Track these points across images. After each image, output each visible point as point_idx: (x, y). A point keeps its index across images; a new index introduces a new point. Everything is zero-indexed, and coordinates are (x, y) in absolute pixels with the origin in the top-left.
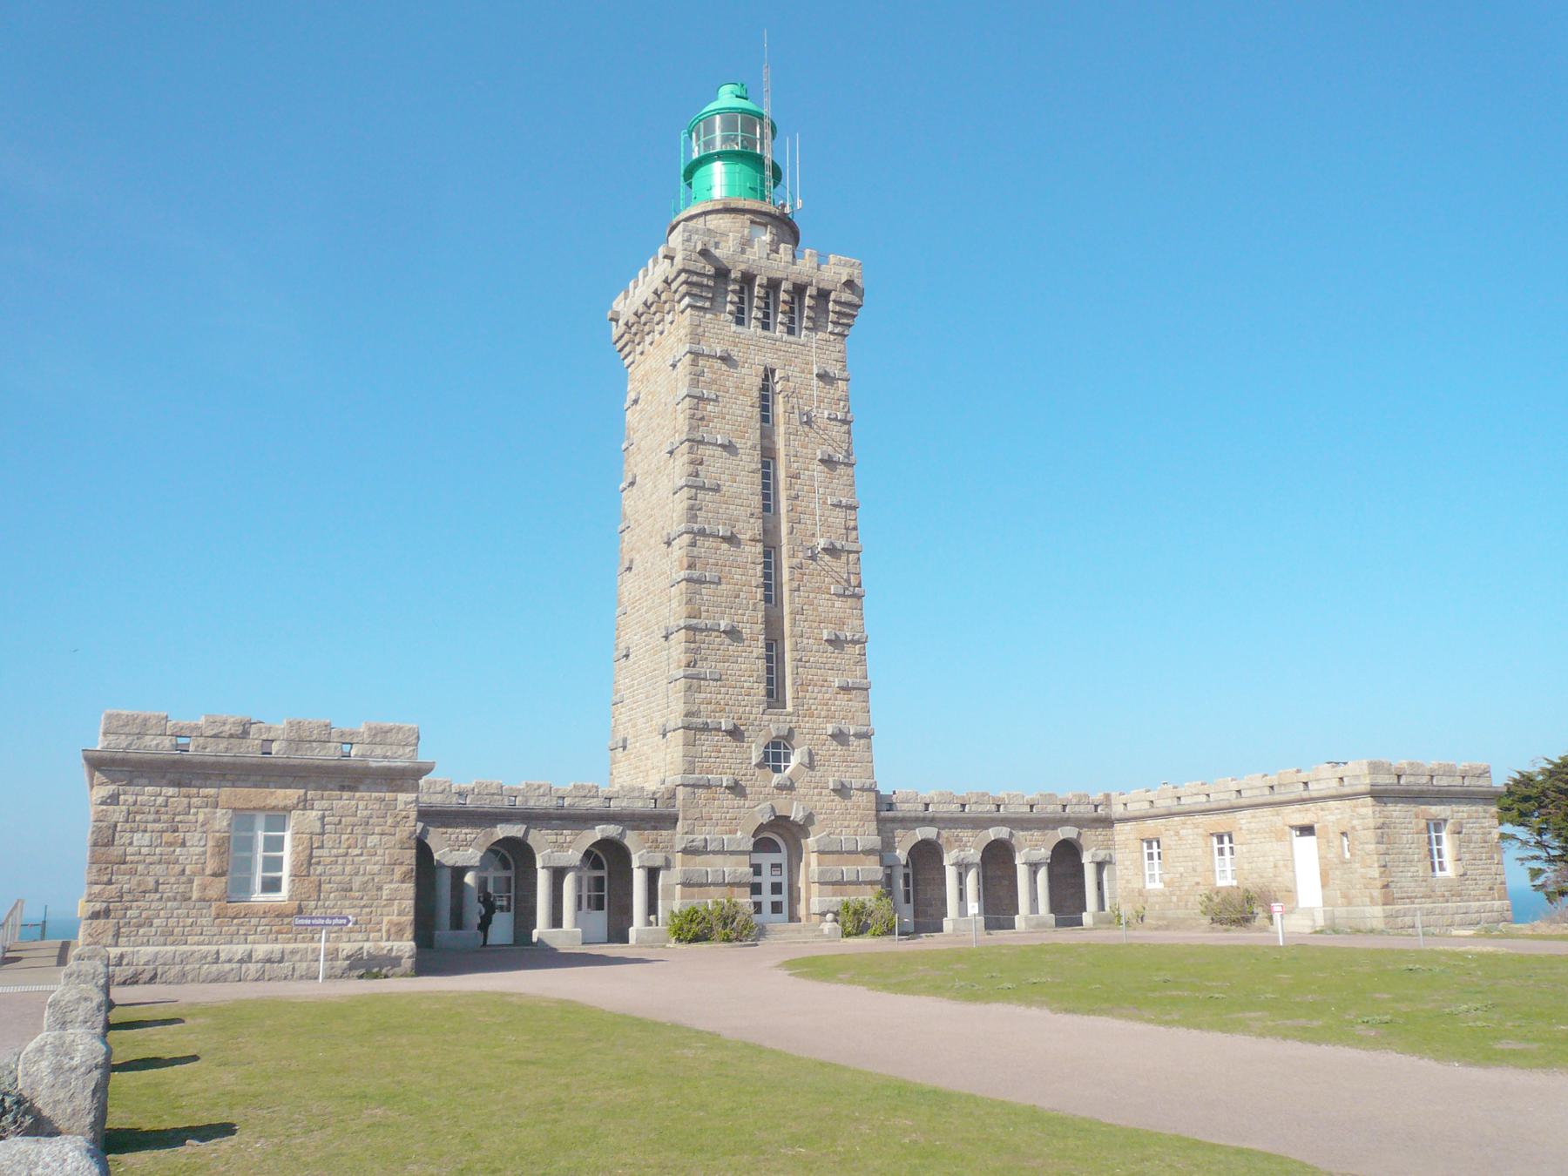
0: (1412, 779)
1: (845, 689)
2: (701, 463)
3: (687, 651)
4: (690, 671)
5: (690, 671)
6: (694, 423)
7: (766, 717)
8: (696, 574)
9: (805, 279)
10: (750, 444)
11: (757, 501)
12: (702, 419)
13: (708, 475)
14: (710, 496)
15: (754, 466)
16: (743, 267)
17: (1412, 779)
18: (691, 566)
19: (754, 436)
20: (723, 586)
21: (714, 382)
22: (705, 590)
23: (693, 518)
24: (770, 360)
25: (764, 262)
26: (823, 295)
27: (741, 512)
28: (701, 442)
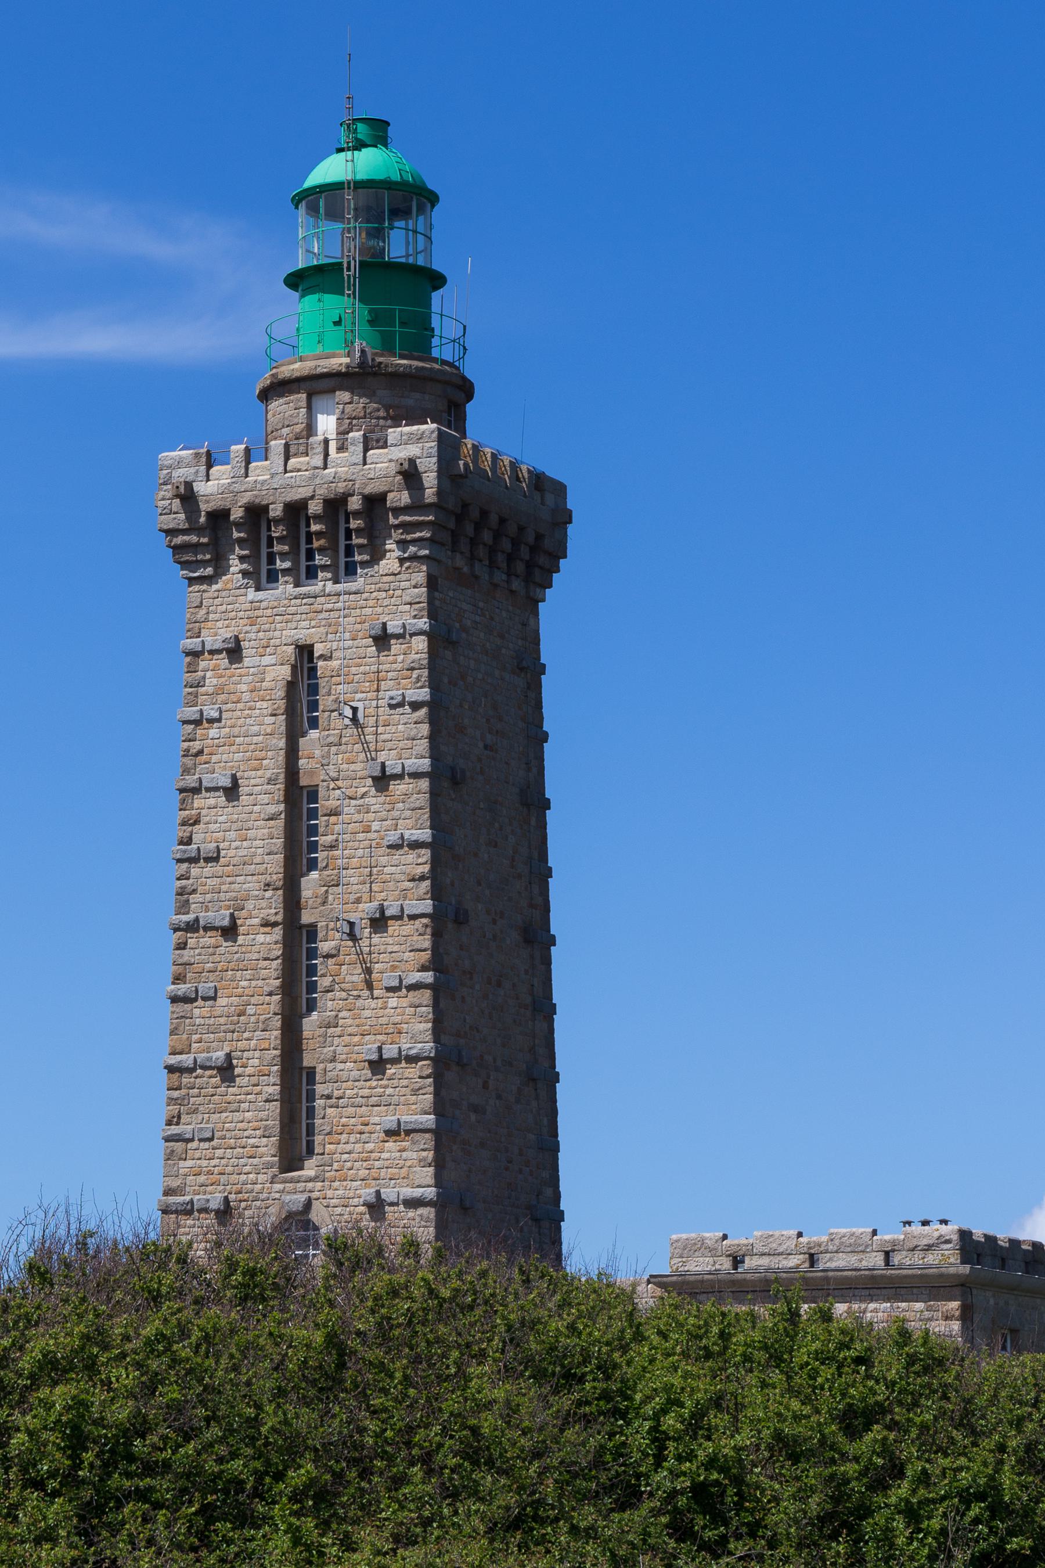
0: (764, 1261)
1: (391, 1133)
2: (197, 822)
3: (171, 1101)
4: (174, 1130)
5: (174, 1130)
6: (189, 761)
7: (278, 1187)
8: (182, 989)
9: (341, 488)
10: (268, 774)
11: (275, 866)
12: (200, 752)
13: (203, 839)
14: (209, 869)
15: (272, 809)
16: (245, 499)
17: (764, 1261)
18: (178, 979)
19: (274, 764)
20: (222, 1001)
21: (219, 690)
22: (199, 1011)
23: (183, 907)
24: (304, 633)
25: (277, 483)
26: (375, 502)
27: (252, 885)
28: (196, 791)
